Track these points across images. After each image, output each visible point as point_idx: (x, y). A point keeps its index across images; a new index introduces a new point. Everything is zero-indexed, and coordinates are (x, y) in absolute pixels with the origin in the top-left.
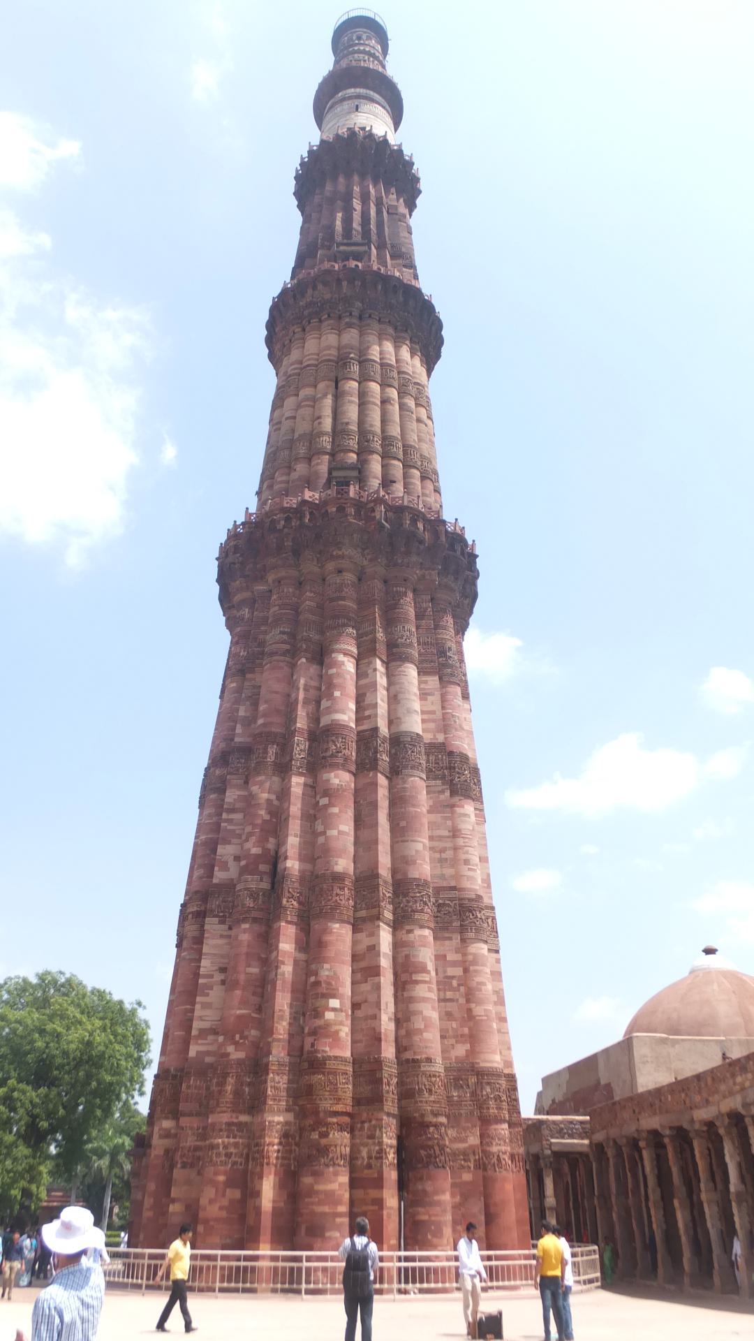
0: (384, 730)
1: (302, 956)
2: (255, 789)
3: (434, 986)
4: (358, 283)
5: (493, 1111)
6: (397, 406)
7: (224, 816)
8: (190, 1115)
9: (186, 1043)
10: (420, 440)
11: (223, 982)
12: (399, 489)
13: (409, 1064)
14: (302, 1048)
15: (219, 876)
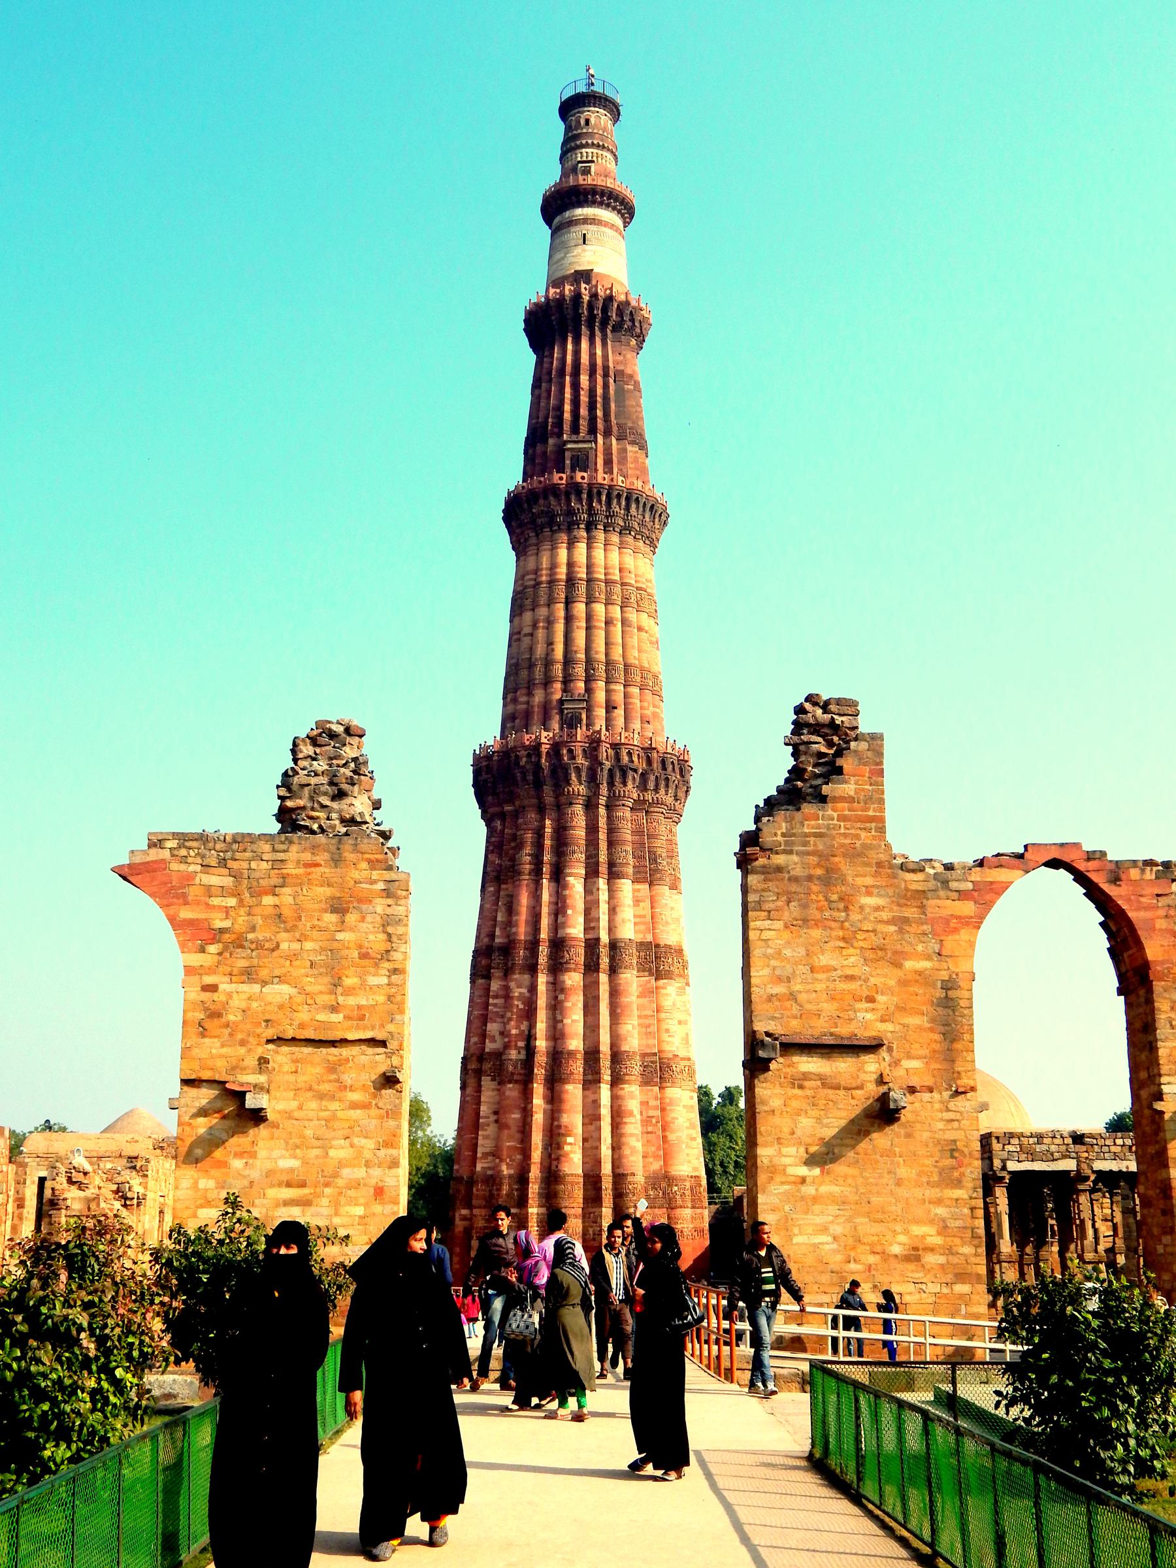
0: (604, 938)
1: (549, 1107)
2: (512, 985)
3: (639, 1125)
4: (585, 496)
5: (679, 1202)
6: (619, 624)
7: (491, 1001)
8: (480, 1207)
9: (474, 1160)
10: (639, 651)
11: (496, 1121)
12: (619, 713)
13: (619, 1178)
14: (550, 1167)
15: (490, 1046)
